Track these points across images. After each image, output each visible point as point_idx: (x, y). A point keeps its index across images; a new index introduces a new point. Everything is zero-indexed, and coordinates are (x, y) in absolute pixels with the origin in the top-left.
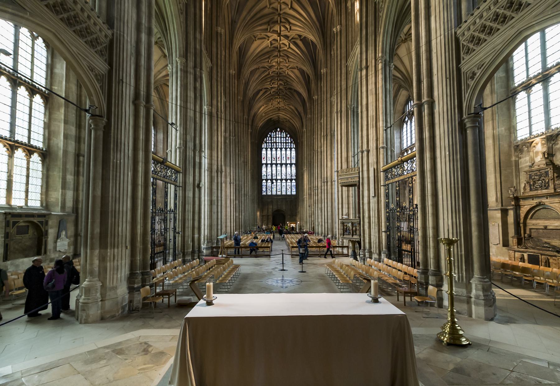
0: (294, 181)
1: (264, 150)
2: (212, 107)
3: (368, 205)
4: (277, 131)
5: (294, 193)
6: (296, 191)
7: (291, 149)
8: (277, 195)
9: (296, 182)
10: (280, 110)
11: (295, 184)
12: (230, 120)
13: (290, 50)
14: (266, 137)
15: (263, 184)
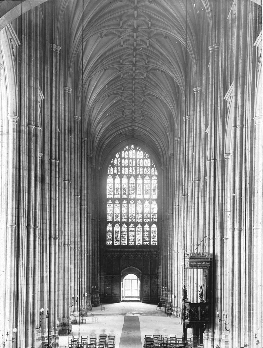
0: (154, 226)
1: (110, 177)
2: (44, 153)
3: (239, 297)
4: (131, 149)
5: (154, 243)
6: (158, 241)
7: (151, 177)
8: (128, 246)
9: (158, 227)
10: (134, 120)
11: (156, 229)
12: (68, 175)
13: (150, 49)
14: (114, 157)
15: (108, 229)
